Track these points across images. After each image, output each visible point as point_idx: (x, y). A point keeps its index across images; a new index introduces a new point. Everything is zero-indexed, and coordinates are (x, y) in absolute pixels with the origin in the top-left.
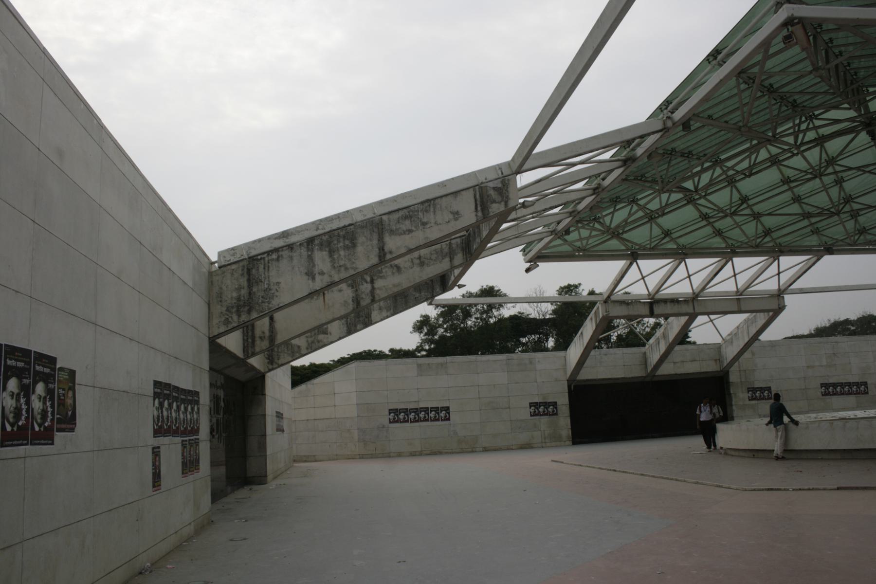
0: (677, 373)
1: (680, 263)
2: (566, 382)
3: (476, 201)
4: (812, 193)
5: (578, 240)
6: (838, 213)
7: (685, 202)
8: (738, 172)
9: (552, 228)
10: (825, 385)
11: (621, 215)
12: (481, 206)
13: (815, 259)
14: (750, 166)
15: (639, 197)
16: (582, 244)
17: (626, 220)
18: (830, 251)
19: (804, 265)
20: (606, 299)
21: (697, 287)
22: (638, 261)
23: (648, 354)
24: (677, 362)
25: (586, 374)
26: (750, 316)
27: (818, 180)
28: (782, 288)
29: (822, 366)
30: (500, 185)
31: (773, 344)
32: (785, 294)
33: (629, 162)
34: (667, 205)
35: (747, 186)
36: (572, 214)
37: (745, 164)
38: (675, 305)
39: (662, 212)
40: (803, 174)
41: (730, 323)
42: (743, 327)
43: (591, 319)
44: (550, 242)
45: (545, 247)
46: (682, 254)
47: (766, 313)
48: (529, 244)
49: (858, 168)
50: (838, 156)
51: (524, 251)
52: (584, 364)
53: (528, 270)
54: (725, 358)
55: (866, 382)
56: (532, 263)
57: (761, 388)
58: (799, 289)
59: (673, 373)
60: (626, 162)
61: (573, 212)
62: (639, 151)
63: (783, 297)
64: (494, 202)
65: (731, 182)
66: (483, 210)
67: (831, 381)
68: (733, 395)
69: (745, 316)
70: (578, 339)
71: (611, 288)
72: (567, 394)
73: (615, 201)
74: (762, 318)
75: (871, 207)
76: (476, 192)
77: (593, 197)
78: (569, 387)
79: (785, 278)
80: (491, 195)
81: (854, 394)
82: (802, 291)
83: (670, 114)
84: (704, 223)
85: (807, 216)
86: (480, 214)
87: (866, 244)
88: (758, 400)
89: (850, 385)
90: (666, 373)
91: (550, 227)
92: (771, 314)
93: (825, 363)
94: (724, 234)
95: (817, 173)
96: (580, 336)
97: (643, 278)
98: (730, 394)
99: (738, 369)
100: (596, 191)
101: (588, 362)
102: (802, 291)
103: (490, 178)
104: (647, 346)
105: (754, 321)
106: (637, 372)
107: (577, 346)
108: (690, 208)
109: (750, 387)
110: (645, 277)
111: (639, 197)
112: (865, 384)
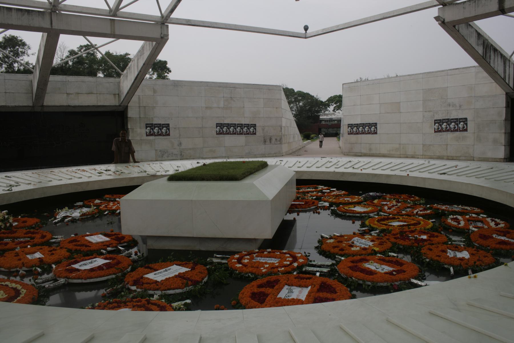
0: (70, 105)
10: (220, 125)
24: (71, 94)
29: (219, 108)
38: (23, 15)
54: (122, 92)
55: (255, 125)
57: (160, 124)
58: (186, 20)
59: (65, 104)
63: (167, 26)
67: (226, 122)
68: (130, 130)
81: (244, 134)
88: (155, 135)
89: (241, 126)
93: (222, 105)
109: (148, 123)
112: (254, 126)
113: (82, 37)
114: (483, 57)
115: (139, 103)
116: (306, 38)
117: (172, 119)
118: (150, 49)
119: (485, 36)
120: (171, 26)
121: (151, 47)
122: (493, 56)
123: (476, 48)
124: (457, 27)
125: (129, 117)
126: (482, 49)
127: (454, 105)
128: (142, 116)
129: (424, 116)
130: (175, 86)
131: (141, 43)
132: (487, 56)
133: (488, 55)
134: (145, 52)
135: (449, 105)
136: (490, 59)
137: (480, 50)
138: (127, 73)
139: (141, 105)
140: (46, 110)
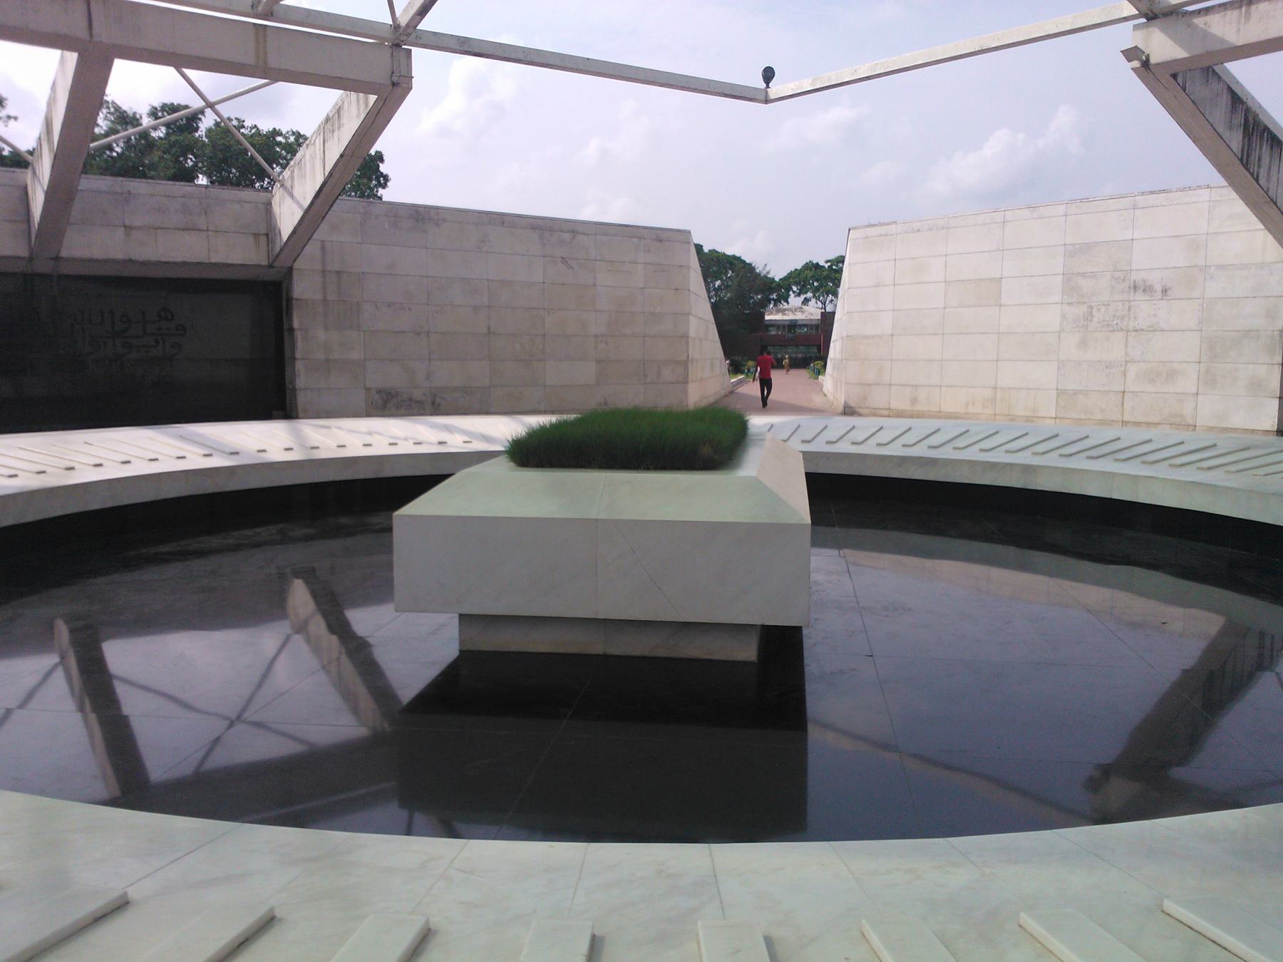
0: (132, 257)
24: (135, 228)
59: (120, 256)
99: (319, 267)
113: (168, 72)
114: (1241, 160)
115: (323, 263)
117: (410, 309)
118: (359, 115)
119: (1250, 104)
120: (417, 52)
121: (362, 107)
122: (1268, 159)
123: (1226, 135)
124: (1180, 80)
125: (297, 299)
126: (1241, 138)
127: (1148, 289)
128: (331, 297)
129: (1064, 316)
130: (417, 220)
131: (334, 95)
132: (1252, 158)
133: (1254, 157)
134: (344, 120)
135: (1135, 288)
136: (1259, 166)
137: (1236, 140)
138: (292, 177)
139: (329, 268)
140: (66, 270)
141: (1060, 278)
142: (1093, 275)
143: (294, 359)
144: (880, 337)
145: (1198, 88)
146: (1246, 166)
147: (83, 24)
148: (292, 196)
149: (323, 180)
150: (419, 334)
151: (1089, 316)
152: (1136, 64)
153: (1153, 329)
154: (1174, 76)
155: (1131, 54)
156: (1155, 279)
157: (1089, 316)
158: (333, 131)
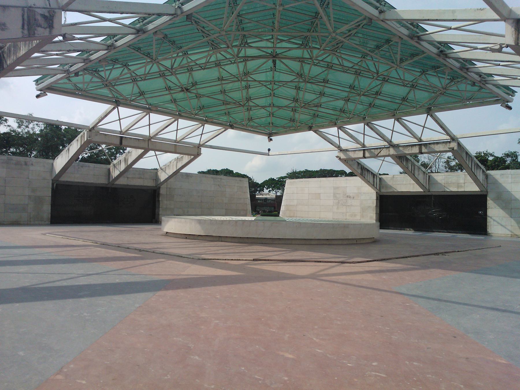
0: (128, 184)
1: (146, 115)
2: (51, 180)
3: (23, 19)
4: (232, 90)
5: (81, 83)
6: (243, 106)
7: (159, 76)
8: (197, 64)
9: (66, 67)
11: (116, 73)
12: (28, 26)
13: (224, 129)
14: (206, 63)
15: (130, 64)
16: (84, 86)
17: (118, 78)
18: (232, 127)
19: (216, 132)
20: (91, 129)
21: (152, 133)
22: (119, 107)
23: (111, 170)
24: (129, 178)
25: (65, 178)
26: (180, 156)
27: (239, 82)
28: (201, 143)
30: (47, 14)
31: (188, 175)
32: (202, 147)
33: (141, 32)
34: (148, 73)
35: (199, 75)
36: (86, 61)
37: (203, 61)
39: (145, 77)
40: (232, 77)
41: (167, 158)
42: (174, 162)
43: (77, 140)
44: (61, 78)
45: (55, 82)
46: (149, 109)
47: (189, 156)
48: (44, 77)
49: (259, 81)
50: (255, 71)
51: (37, 82)
52: (66, 170)
53: (38, 96)
56: (42, 92)
60: (139, 31)
61: (87, 59)
62: (151, 27)
64: (40, 26)
65: (190, 70)
66: (29, 30)
69: (176, 156)
70: (65, 153)
71: (96, 122)
72: (51, 189)
73: (115, 61)
74: (186, 159)
75: (258, 106)
76: (24, 12)
77: (106, 52)
78: (53, 184)
79: (205, 137)
80: (38, 20)
82: (211, 147)
83: (180, 5)
84: (167, 92)
85: (225, 103)
86: (26, 32)
87: (252, 127)
90: (121, 183)
91: (65, 67)
92: (192, 157)
94: (177, 103)
95: (238, 79)
96: (66, 151)
97: (120, 120)
98: (159, 201)
99: (166, 187)
100: (109, 48)
101: (69, 170)
102: (211, 147)
103: (38, 5)
104: (112, 165)
105: (177, 159)
106: (102, 181)
107: (63, 157)
108: (161, 80)
110: (121, 119)
111: (130, 64)
114: (361, 174)
115: (167, 186)
116: (269, 155)
118: (188, 159)
119: (362, 164)
123: (357, 170)
127: (350, 197)
129: (334, 202)
132: (363, 174)
133: (364, 173)
135: (348, 197)
141: (332, 194)
142: (339, 194)
143: (159, 207)
144: (294, 205)
145: (350, 162)
146: (362, 175)
147: (147, 145)
148: (165, 172)
149: (176, 170)
150: (186, 202)
151: (339, 203)
152: (338, 158)
153: (351, 205)
154: (345, 161)
155: (337, 157)
156: (351, 195)
157: (339, 203)
158: (180, 161)
